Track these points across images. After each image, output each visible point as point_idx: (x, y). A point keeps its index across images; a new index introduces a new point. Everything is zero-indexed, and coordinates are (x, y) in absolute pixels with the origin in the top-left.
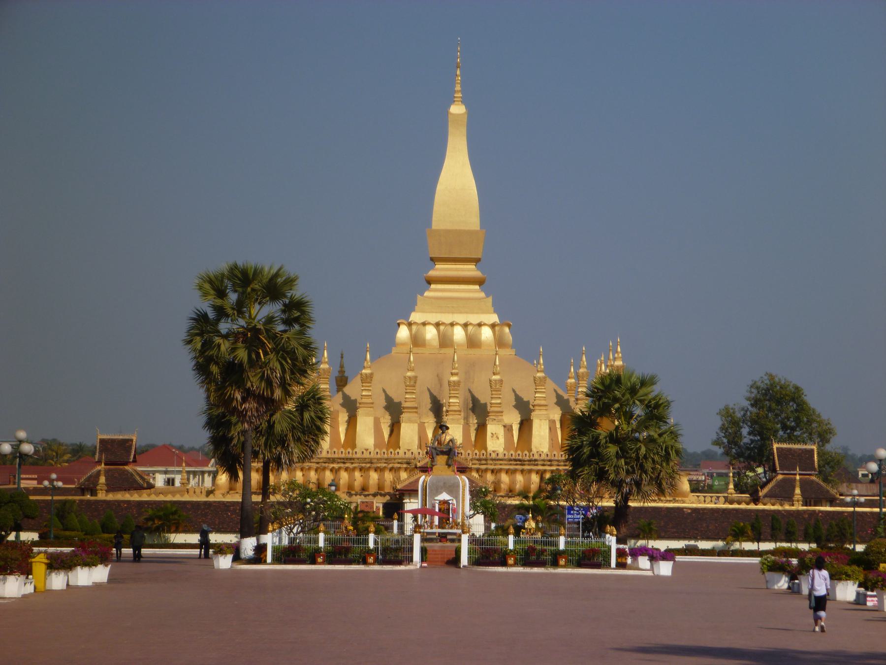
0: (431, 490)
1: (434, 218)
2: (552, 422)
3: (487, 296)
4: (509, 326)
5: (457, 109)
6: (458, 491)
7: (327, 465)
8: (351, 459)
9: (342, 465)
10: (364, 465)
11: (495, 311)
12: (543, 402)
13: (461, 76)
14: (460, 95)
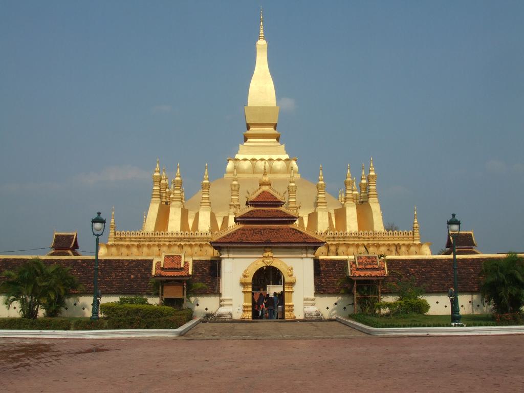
1: (249, 99)
2: (330, 214)
3: (281, 144)
5: (262, 43)
7: (176, 243)
8: (194, 238)
9: (187, 243)
10: (202, 243)
11: (287, 153)
12: (324, 201)
14: (263, 35)
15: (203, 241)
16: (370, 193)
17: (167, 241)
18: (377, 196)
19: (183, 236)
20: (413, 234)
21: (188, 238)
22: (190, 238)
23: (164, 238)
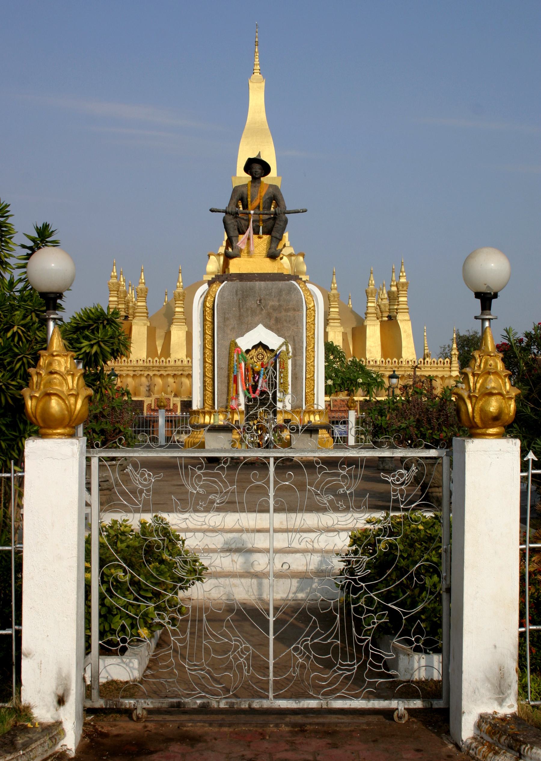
0: (225, 319)
4: (303, 256)
6: (296, 322)
7: (142, 373)
8: (165, 367)
9: (157, 373)
10: (176, 373)
13: (258, 52)
14: (258, 67)
15: (178, 371)
16: (400, 306)
17: (131, 371)
18: (409, 311)
19: (151, 364)
20: (451, 363)
21: (157, 367)
22: (160, 367)
23: (127, 367)
